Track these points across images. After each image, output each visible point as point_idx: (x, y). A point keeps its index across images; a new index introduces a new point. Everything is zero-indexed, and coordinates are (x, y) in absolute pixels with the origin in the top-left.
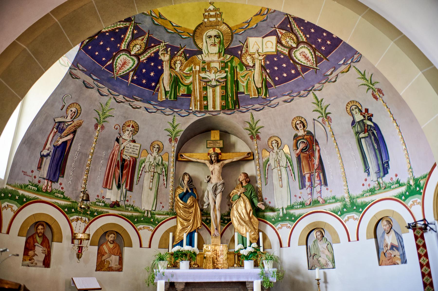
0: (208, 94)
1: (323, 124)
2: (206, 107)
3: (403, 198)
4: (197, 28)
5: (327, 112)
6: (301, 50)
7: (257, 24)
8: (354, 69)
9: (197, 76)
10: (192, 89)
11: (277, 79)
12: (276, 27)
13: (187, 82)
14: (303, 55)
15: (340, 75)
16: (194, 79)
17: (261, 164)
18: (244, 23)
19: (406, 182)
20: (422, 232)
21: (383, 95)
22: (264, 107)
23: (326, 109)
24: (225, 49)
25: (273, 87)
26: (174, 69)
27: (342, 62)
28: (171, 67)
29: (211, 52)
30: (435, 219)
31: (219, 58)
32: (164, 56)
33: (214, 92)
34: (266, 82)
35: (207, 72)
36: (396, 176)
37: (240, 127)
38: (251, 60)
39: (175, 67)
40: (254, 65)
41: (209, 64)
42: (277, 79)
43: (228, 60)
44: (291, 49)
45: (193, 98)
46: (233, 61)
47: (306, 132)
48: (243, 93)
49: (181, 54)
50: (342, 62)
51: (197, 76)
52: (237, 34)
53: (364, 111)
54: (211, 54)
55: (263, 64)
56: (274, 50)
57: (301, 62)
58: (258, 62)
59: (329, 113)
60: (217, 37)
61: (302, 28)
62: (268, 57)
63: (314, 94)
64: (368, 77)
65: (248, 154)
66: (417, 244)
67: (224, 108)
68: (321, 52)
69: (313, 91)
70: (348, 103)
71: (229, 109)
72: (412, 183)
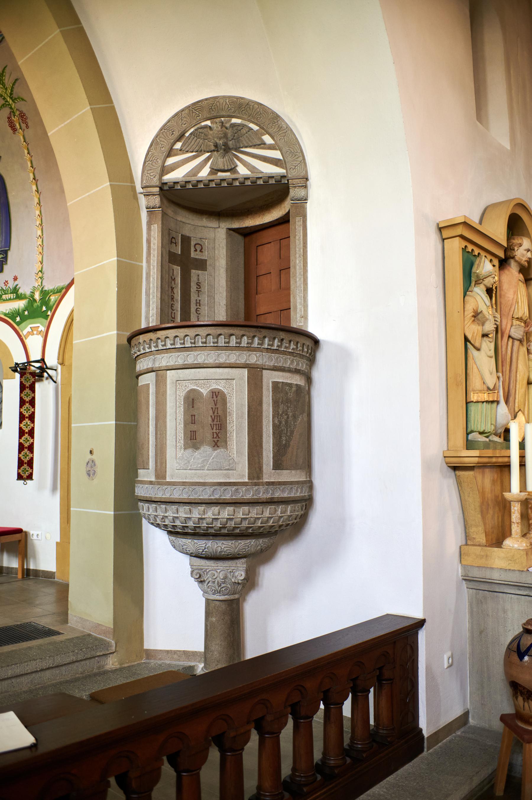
3: (18, 319)
19: (28, 293)
20: (33, 380)
21: (27, 127)
30: (58, 362)
36: (15, 279)
66: (21, 398)
72: (37, 296)
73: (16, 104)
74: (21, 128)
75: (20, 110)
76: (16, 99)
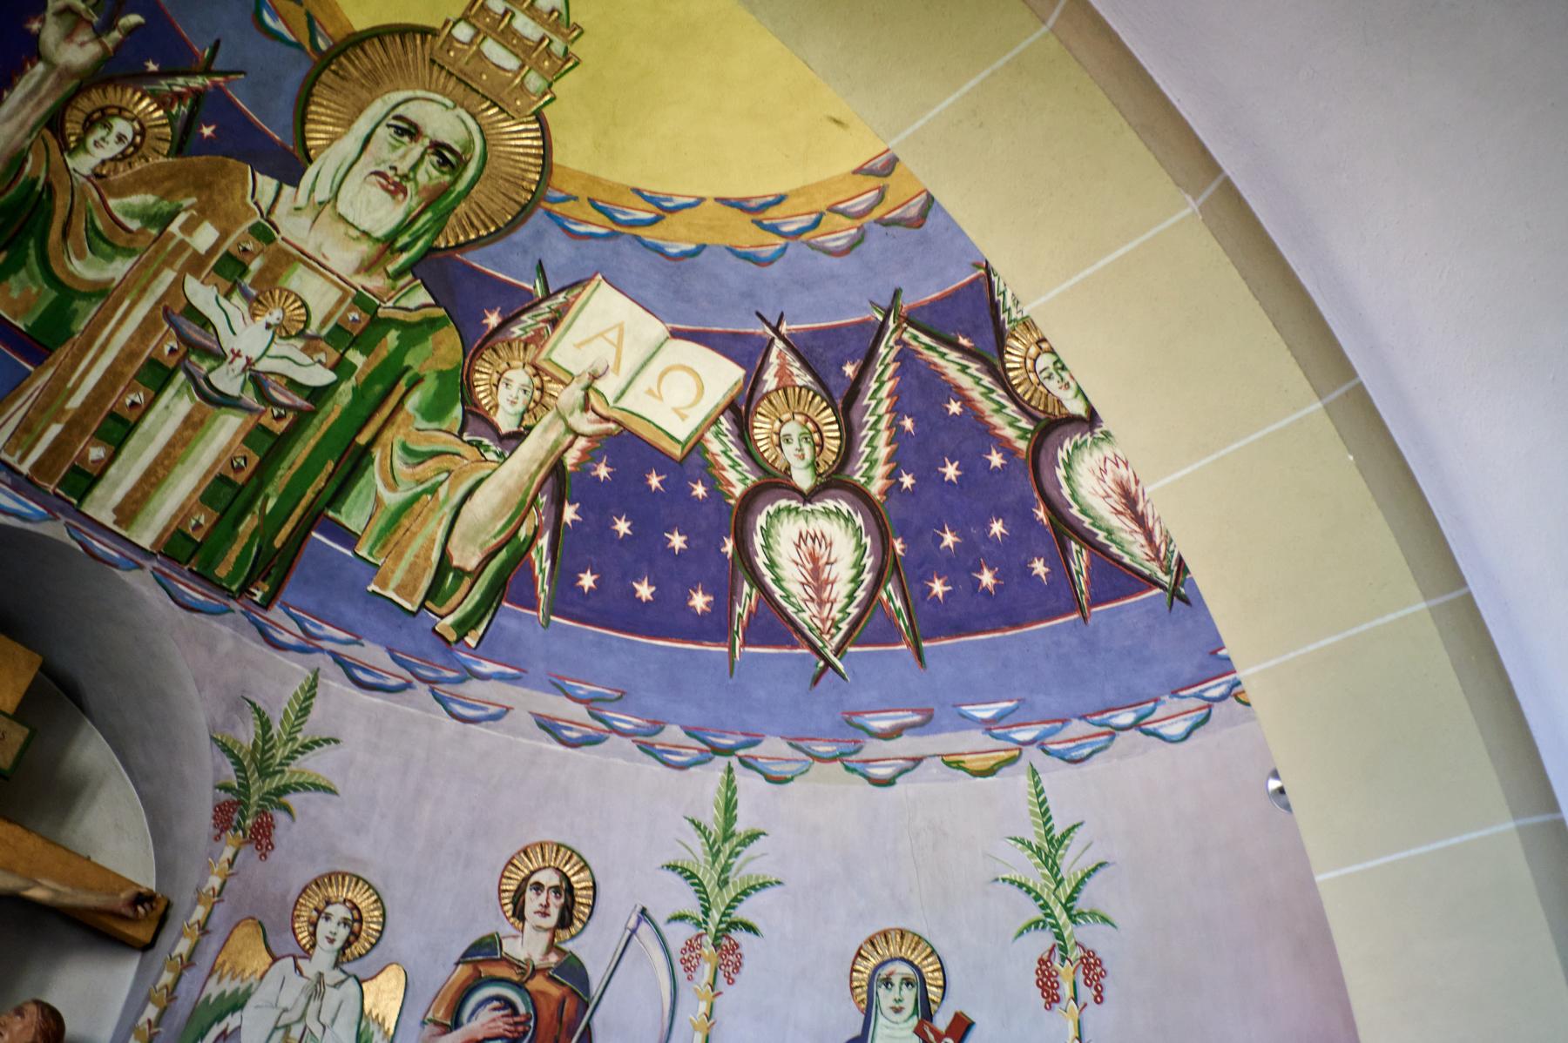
0: (151, 417)
1: (679, 968)
2: (85, 480)
4: (380, 34)
5: (742, 912)
6: (821, 525)
7: (701, 248)
8: (1025, 780)
9: (168, 276)
10: (80, 326)
11: (587, 581)
12: (784, 329)
13: (85, 269)
14: (814, 554)
15: (933, 767)
16: (136, 285)
17: (183, 1007)
18: (638, 191)
21: (1099, 998)
22: (409, 685)
23: (745, 893)
24: (431, 250)
25: (535, 608)
26: (64, 148)
27: (985, 712)
28: (54, 122)
29: (344, 207)
31: (358, 272)
32: (69, 36)
33: (193, 426)
34: (520, 558)
35: (236, 298)
37: (200, 712)
38: (522, 399)
39: (81, 142)
40: (518, 437)
41: (286, 258)
42: (587, 581)
43: (400, 315)
44: (773, 483)
45: (41, 382)
46: (421, 339)
47: (553, 958)
48: (349, 538)
49: (180, 97)
50: (985, 712)
51: (168, 276)
52: (559, 221)
53: (942, 1021)
54: (342, 218)
55: (571, 458)
56: (682, 431)
57: (778, 580)
58: (552, 436)
59: (750, 928)
60: (445, 161)
61: (908, 423)
62: (626, 446)
63: (729, 783)
64: (1071, 863)
65: (142, 898)
67: (182, 551)
68: (916, 598)
69: (734, 761)
70: (885, 934)
71: (204, 577)
73: (1080, 929)
74: (1075, 999)
75: (1088, 947)
76: (1081, 914)
